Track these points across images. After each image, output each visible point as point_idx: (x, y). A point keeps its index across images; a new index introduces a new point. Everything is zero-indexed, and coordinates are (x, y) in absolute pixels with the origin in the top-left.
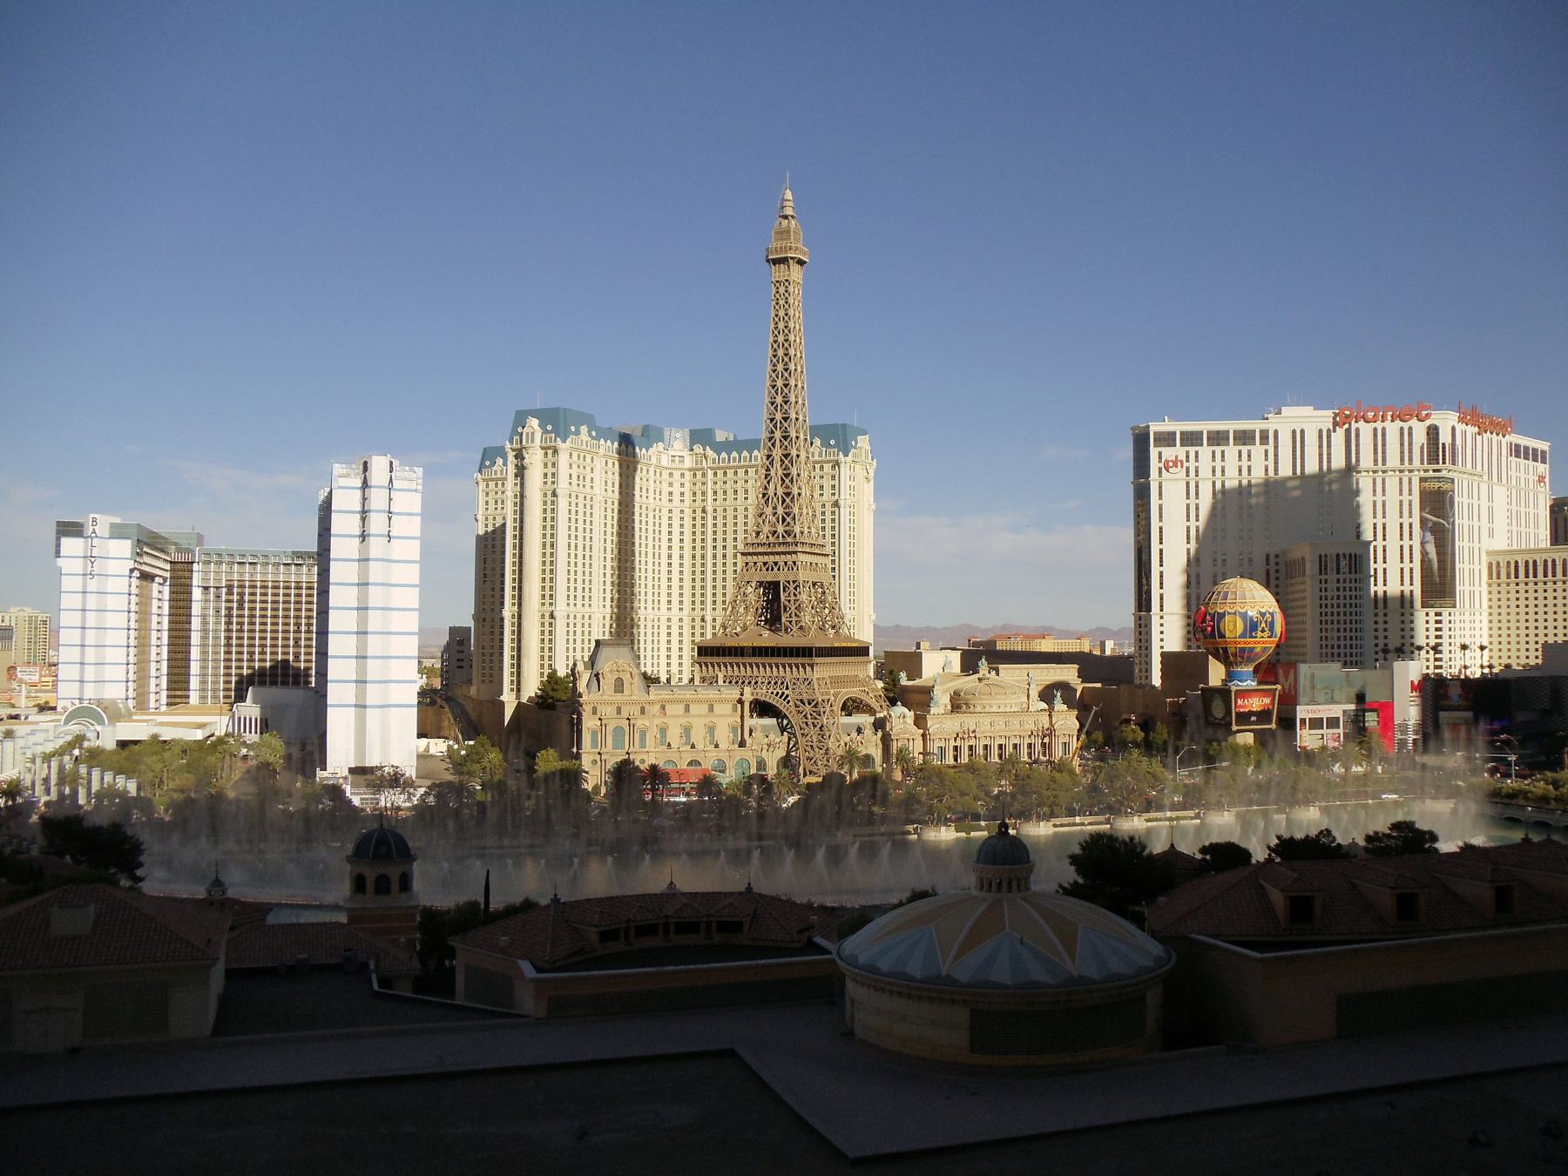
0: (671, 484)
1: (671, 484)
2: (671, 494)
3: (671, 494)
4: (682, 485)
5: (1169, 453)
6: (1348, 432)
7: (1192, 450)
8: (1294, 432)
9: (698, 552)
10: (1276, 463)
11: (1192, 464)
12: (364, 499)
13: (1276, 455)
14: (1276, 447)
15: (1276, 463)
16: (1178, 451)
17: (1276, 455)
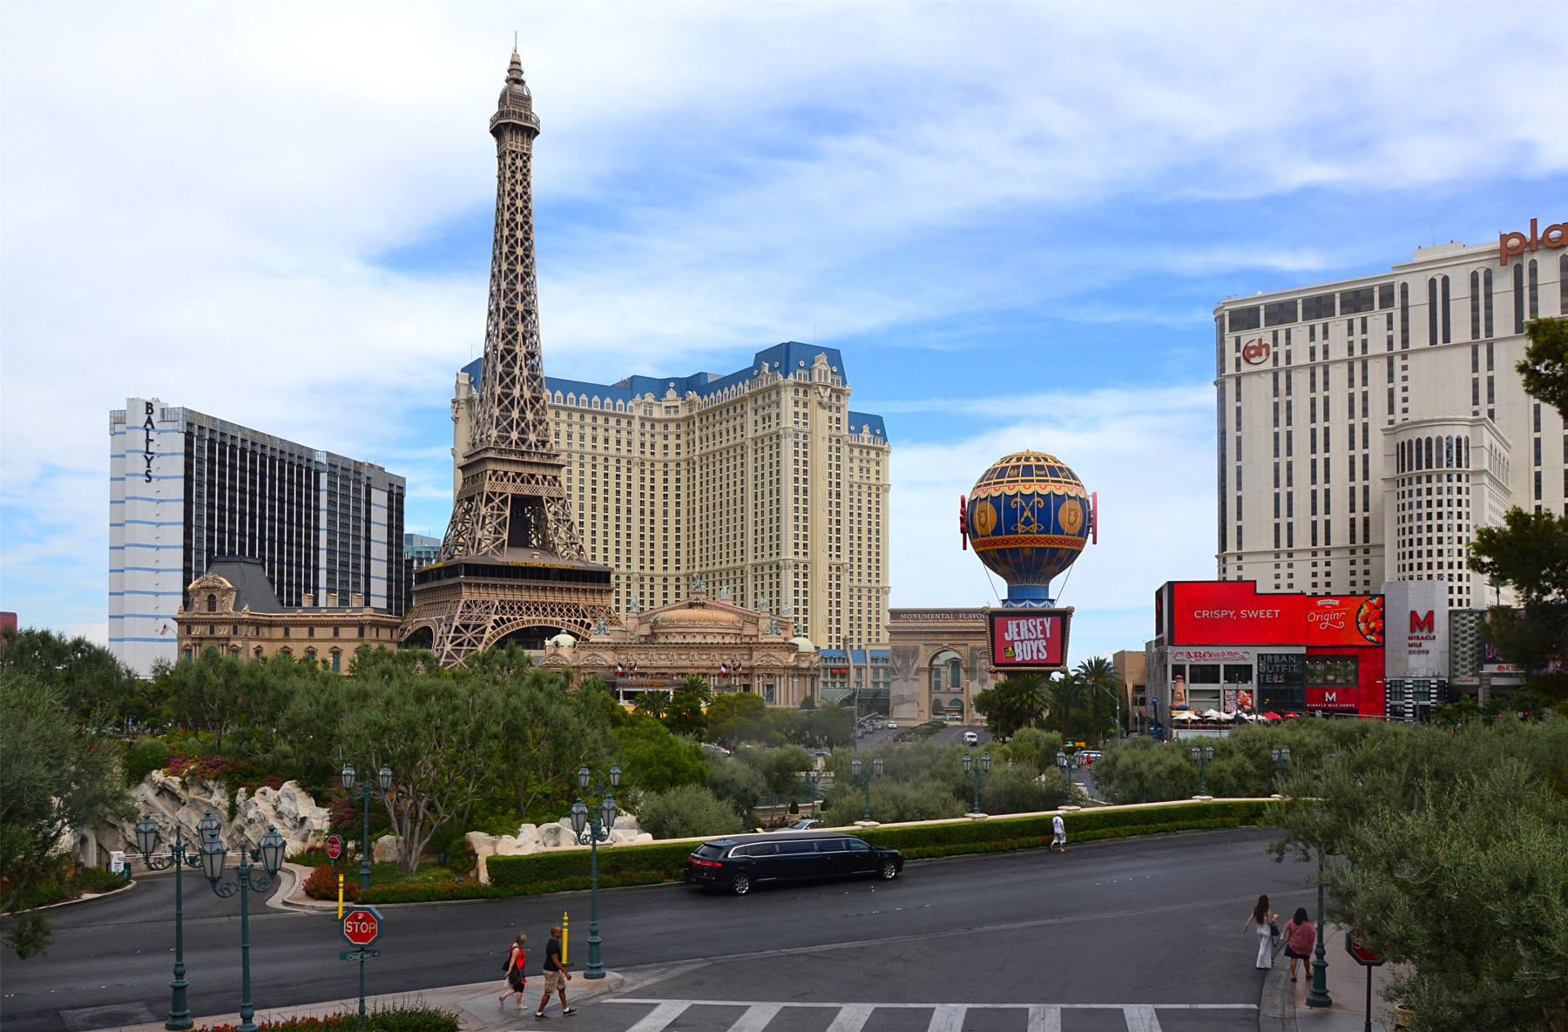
0: (666, 437)
1: (666, 437)
2: (666, 447)
3: (666, 447)
4: (678, 437)
5: (1247, 337)
6: (1518, 271)
7: (1281, 330)
8: (1432, 282)
9: (647, 508)
10: (1405, 330)
11: (1282, 349)
12: (148, 441)
13: (1405, 320)
14: (1405, 309)
15: (1405, 330)
16: (1264, 334)
17: (1405, 320)
